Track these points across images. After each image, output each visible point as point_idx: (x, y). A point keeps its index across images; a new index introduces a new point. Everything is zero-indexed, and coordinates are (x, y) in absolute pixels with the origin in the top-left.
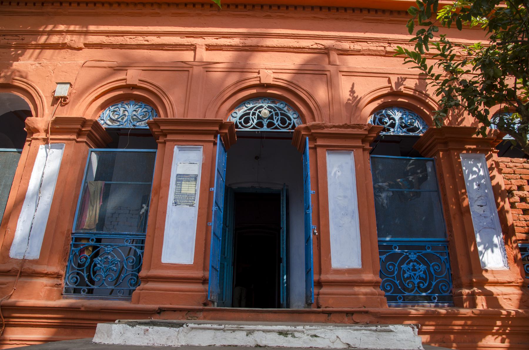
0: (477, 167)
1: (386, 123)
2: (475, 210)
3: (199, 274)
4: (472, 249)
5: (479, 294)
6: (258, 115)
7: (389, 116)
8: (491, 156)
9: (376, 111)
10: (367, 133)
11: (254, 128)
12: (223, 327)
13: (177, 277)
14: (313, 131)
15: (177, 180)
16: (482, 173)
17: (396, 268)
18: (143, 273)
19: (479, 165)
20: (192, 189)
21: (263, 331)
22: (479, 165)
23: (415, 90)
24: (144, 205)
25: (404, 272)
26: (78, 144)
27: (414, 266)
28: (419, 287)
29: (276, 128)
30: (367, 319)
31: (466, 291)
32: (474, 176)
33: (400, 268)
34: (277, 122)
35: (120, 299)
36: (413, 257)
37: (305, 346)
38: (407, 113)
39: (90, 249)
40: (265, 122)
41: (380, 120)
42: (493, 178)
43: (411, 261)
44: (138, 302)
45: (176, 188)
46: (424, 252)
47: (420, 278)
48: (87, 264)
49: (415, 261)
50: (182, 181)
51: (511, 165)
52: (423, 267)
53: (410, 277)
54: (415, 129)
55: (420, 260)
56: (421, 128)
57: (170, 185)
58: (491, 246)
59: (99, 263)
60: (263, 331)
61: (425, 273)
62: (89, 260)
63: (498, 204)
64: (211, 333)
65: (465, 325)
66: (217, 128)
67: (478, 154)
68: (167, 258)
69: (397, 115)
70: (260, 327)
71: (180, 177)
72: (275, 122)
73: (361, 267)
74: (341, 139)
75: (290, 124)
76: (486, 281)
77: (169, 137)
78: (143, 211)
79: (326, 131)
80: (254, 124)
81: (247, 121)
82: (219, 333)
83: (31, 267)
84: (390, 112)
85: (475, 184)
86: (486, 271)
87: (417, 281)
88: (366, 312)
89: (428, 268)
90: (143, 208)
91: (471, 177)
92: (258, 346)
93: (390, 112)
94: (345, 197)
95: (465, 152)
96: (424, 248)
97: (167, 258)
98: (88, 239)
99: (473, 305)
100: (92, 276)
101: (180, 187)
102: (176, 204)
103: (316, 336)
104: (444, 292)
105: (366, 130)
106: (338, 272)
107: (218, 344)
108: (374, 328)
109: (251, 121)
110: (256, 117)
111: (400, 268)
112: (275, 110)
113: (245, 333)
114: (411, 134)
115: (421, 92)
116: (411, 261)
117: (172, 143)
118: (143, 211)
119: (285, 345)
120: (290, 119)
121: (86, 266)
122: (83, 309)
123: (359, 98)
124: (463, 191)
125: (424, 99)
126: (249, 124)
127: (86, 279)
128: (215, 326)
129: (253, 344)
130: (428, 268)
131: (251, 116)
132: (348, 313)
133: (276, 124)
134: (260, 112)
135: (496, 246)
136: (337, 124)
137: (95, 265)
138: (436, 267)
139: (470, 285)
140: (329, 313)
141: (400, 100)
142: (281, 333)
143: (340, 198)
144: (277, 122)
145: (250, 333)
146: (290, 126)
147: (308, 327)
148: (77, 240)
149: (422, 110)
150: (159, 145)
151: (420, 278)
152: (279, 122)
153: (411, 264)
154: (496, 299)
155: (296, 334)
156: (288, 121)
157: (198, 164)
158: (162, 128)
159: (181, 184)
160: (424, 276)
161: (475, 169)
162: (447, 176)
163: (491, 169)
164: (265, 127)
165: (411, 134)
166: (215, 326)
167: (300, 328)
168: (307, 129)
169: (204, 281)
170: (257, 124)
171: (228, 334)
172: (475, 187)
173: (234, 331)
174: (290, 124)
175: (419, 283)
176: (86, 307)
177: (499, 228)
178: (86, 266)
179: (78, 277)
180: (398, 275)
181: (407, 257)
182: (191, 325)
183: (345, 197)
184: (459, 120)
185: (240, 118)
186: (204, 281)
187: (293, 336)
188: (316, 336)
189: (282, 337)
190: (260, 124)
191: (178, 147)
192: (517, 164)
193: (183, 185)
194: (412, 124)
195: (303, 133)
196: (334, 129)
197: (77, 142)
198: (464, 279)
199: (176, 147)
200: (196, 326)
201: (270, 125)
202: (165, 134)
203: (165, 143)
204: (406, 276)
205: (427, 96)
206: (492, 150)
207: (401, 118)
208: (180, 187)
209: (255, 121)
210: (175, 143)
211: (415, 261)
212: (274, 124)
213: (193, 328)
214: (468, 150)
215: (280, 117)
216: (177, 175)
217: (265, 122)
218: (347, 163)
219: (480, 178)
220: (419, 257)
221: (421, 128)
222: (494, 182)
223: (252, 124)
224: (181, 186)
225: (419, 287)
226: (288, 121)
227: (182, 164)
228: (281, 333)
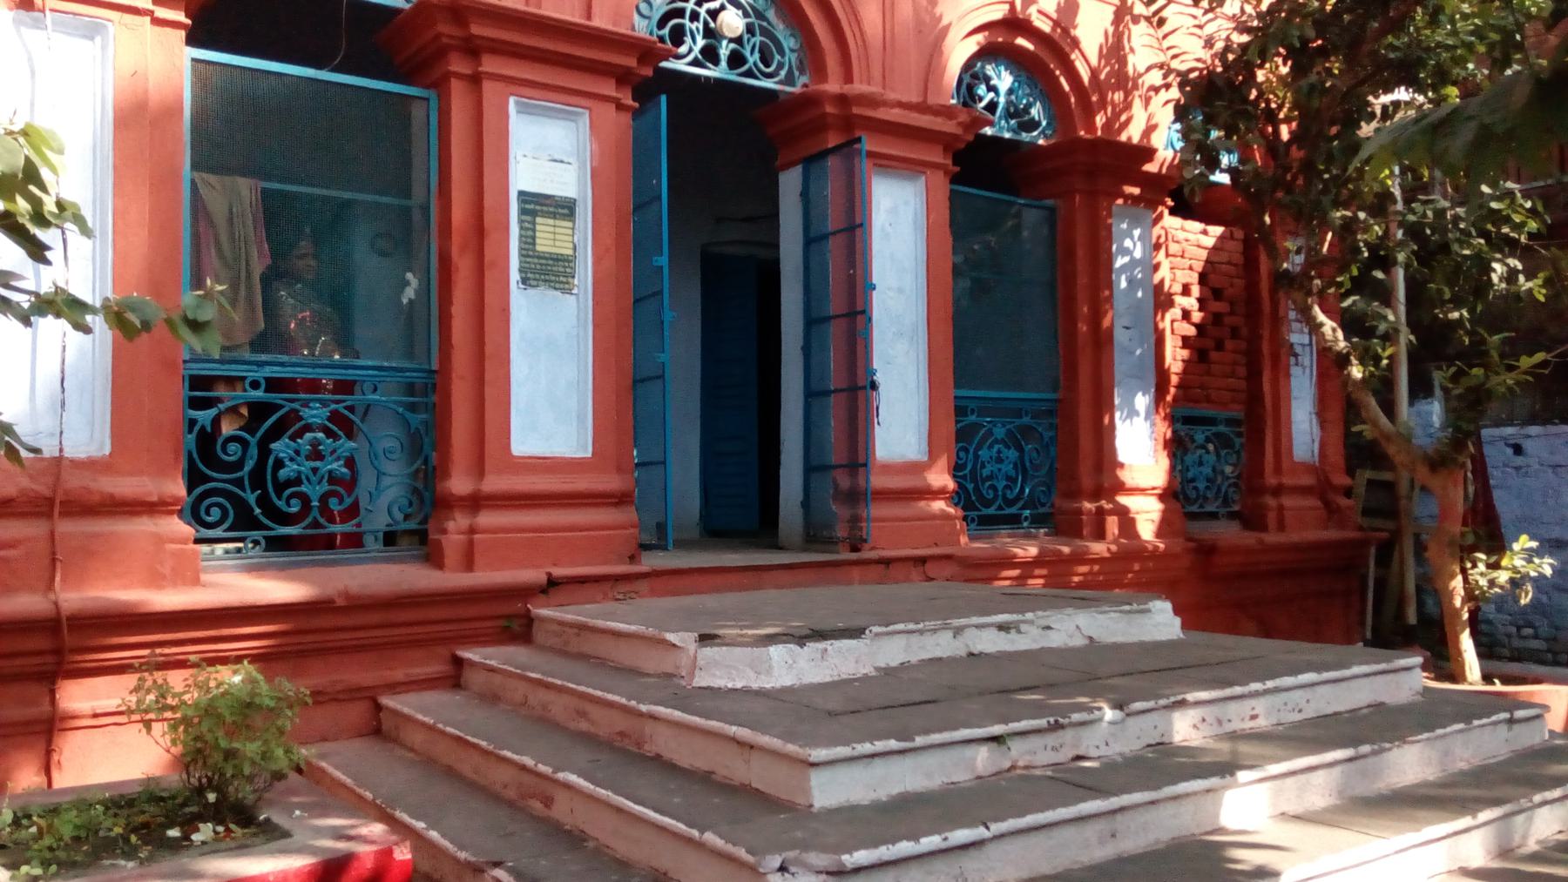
0: (1132, 238)
1: (981, 99)
2: (1120, 336)
3: (610, 482)
4: (1106, 421)
5: (1111, 513)
6: (706, 24)
7: (987, 79)
8: (1160, 216)
9: (968, 65)
10: (959, 131)
11: (696, 63)
12: (921, 626)
13: (551, 490)
14: (856, 110)
15: (523, 212)
16: (1138, 254)
17: (971, 456)
18: (459, 484)
19: (1137, 233)
20: (575, 241)
21: (977, 627)
22: (1137, 233)
23: (1056, 24)
24: (409, 276)
25: (983, 466)
26: (158, 29)
27: (999, 452)
28: (1004, 496)
29: (749, 74)
30: (950, 569)
31: (1088, 506)
32: (1127, 259)
33: (976, 457)
34: (753, 59)
35: (375, 560)
36: (1000, 432)
37: (1035, 646)
38: (1023, 79)
39: (244, 411)
40: (724, 50)
41: (971, 89)
42: (1156, 267)
43: (996, 441)
44: (469, 564)
46: (1018, 422)
47: (1009, 478)
48: (249, 465)
49: (1002, 441)
50: (534, 214)
51: (1181, 235)
52: (1012, 454)
53: (990, 477)
54: (1032, 125)
55: (1013, 440)
56: (1044, 123)
58: (1133, 413)
59: (292, 460)
60: (977, 627)
61: (1015, 465)
62: (254, 451)
63: (1156, 325)
64: (900, 641)
65: (1090, 573)
66: (631, 62)
67: (1140, 210)
68: (522, 445)
69: (1004, 80)
70: (975, 620)
72: (747, 53)
73: (926, 458)
74: (905, 141)
75: (780, 66)
76: (1121, 488)
77: (490, 64)
78: (409, 293)
79: (882, 114)
80: (697, 49)
81: (678, 36)
82: (915, 638)
83: (93, 485)
84: (990, 70)
85: (1123, 277)
86: (1122, 466)
87: (1001, 485)
88: (948, 557)
89: (1022, 458)
90: (408, 283)
91: (1120, 262)
92: (971, 654)
93: (990, 70)
94: (900, 290)
95: (1120, 201)
96: (1018, 414)
97: (522, 445)
98: (231, 381)
99: (1100, 535)
100: (275, 499)
102: (524, 281)
103: (1049, 628)
104: (1043, 505)
105: (959, 124)
106: (888, 468)
107: (914, 659)
108: (1127, 608)
109: (688, 39)
110: (701, 27)
111: (976, 457)
112: (746, 15)
113: (950, 634)
114: (1025, 137)
115: (1066, 31)
116: (996, 441)
117: (499, 86)
118: (409, 293)
119: (1009, 647)
120: (782, 52)
121: (247, 469)
122: (340, 602)
123: (945, 22)
124: (1107, 293)
125: (1067, 49)
126: (683, 49)
127: (258, 511)
128: (911, 626)
129: (963, 653)
130: (1022, 458)
131: (686, 21)
132: (922, 561)
133: (751, 60)
134: (714, 14)
135: (1137, 414)
136: (904, 99)
137: (279, 464)
138: (1034, 455)
139: (1096, 495)
140: (887, 562)
141: (1021, 41)
142: (1003, 627)
143: (891, 294)
144: (753, 59)
145: (958, 631)
146: (783, 73)
147: (1040, 613)
148: (197, 382)
149: (1057, 78)
150: (456, 85)
151: (1009, 478)
152: (757, 55)
153: (996, 447)
154: (1133, 521)
155: (1023, 627)
156: (777, 57)
157: (575, 166)
158: (476, 30)
159: (534, 223)
160: (1012, 473)
161: (1128, 243)
162: (1081, 253)
163: (1157, 247)
164: (724, 64)
165: (1025, 137)
166: (911, 626)
167: (1029, 616)
168: (843, 100)
169: (620, 499)
170: (704, 51)
171: (929, 640)
172: (1124, 284)
173: (935, 631)
174: (780, 66)
175: (1006, 487)
176: (347, 595)
177: (1152, 380)
178: (247, 469)
179: (220, 500)
180: (973, 471)
181: (990, 433)
182: (876, 629)
183: (900, 290)
184: (1123, 118)
185: (662, 23)
186: (620, 499)
187: (1019, 632)
188: (1049, 628)
189: (1003, 634)
190: (710, 54)
191: (517, 103)
192: (1191, 236)
194: (1027, 110)
195: (829, 109)
196: (896, 111)
197: (158, 22)
198: (1087, 482)
199: (512, 100)
200: (884, 629)
201: (736, 60)
202: (473, 49)
203: (475, 80)
204: (986, 472)
205: (1075, 43)
206: (1164, 204)
207: (1010, 91)
209: (701, 42)
210: (513, 88)
211: (1002, 441)
212: (743, 61)
213: (877, 635)
214: (1127, 197)
215: (758, 39)
217: (724, 50)
218: (906, 203)
219: (1134, 263)
220: (1010, 433)
221: (1044, 123)
222: (1157, 278)
223: (690, 50)
224: (534, 230)
225: (1004, 496)
226: (777, 57)
228: (1003, 627)
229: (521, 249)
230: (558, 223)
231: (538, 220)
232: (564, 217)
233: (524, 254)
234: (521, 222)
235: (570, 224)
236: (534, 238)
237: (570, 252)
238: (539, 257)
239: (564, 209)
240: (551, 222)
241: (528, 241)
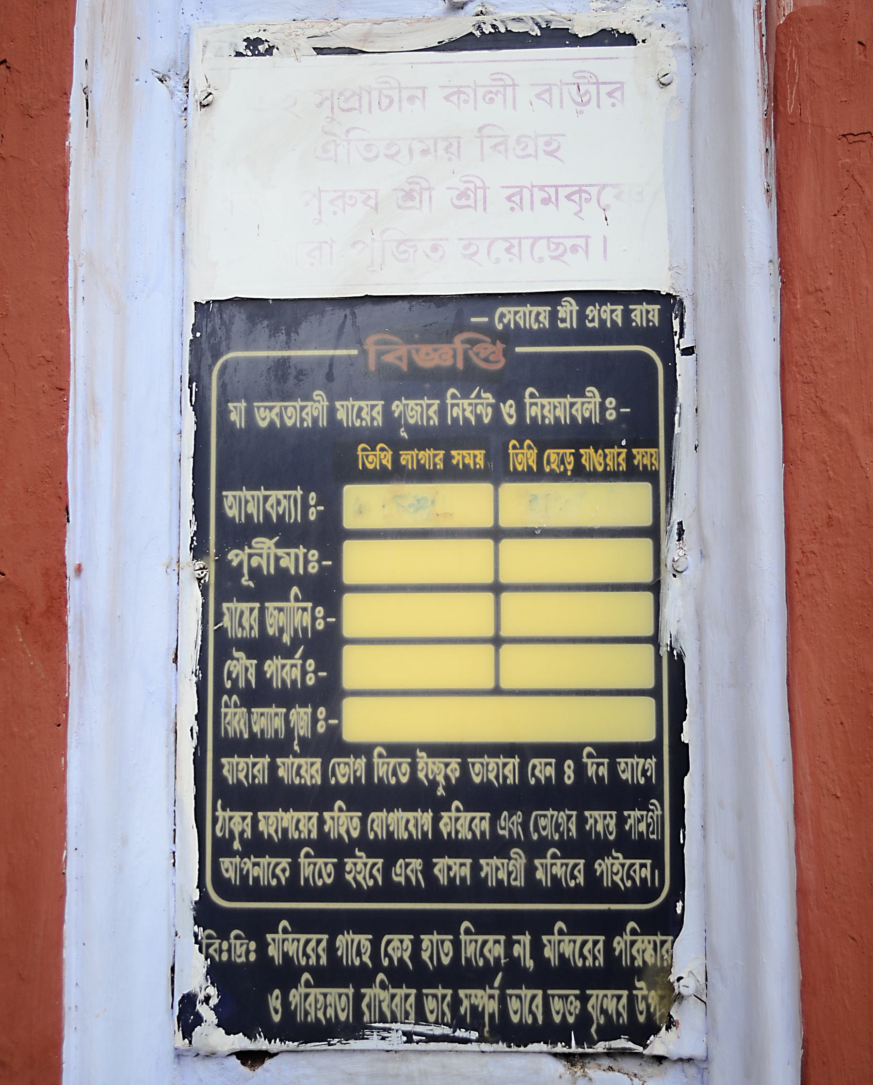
15: (228, 458)
45: (219, 646)
50: (325, 463)
57: (87, 600)
71: (285, 381)
101: (291, 616)
157: (662, 49)
159: (329, 535)
193: (359, 562)
208: (291, 616)
216: (217, 322)
224: (327, 590)
227: (295, 73)
229: (214, 745)
230: (521, 503)
231: (364, 504)
232: (573, 450)
233: (232, 781)
234: (216, 536)
235: (630, 502)
236: (326, 646)
237: (636, 722)
238: (367, 796)
239: (594, 381)
240: (466, 502)
241: (270, 674)
